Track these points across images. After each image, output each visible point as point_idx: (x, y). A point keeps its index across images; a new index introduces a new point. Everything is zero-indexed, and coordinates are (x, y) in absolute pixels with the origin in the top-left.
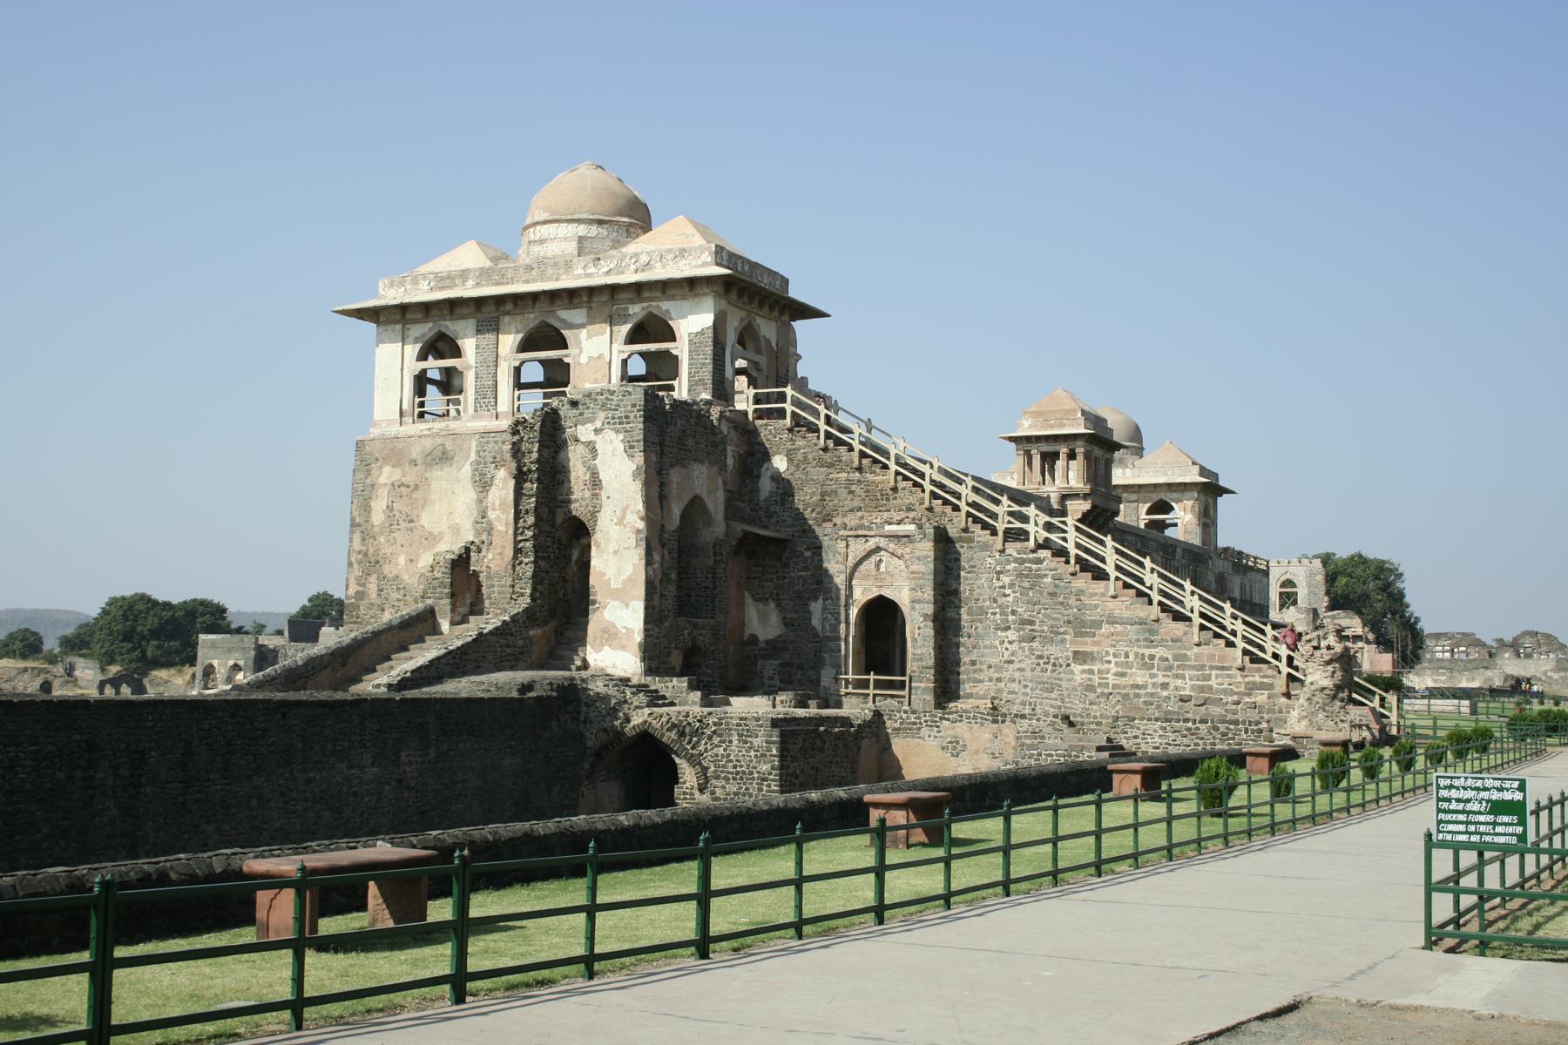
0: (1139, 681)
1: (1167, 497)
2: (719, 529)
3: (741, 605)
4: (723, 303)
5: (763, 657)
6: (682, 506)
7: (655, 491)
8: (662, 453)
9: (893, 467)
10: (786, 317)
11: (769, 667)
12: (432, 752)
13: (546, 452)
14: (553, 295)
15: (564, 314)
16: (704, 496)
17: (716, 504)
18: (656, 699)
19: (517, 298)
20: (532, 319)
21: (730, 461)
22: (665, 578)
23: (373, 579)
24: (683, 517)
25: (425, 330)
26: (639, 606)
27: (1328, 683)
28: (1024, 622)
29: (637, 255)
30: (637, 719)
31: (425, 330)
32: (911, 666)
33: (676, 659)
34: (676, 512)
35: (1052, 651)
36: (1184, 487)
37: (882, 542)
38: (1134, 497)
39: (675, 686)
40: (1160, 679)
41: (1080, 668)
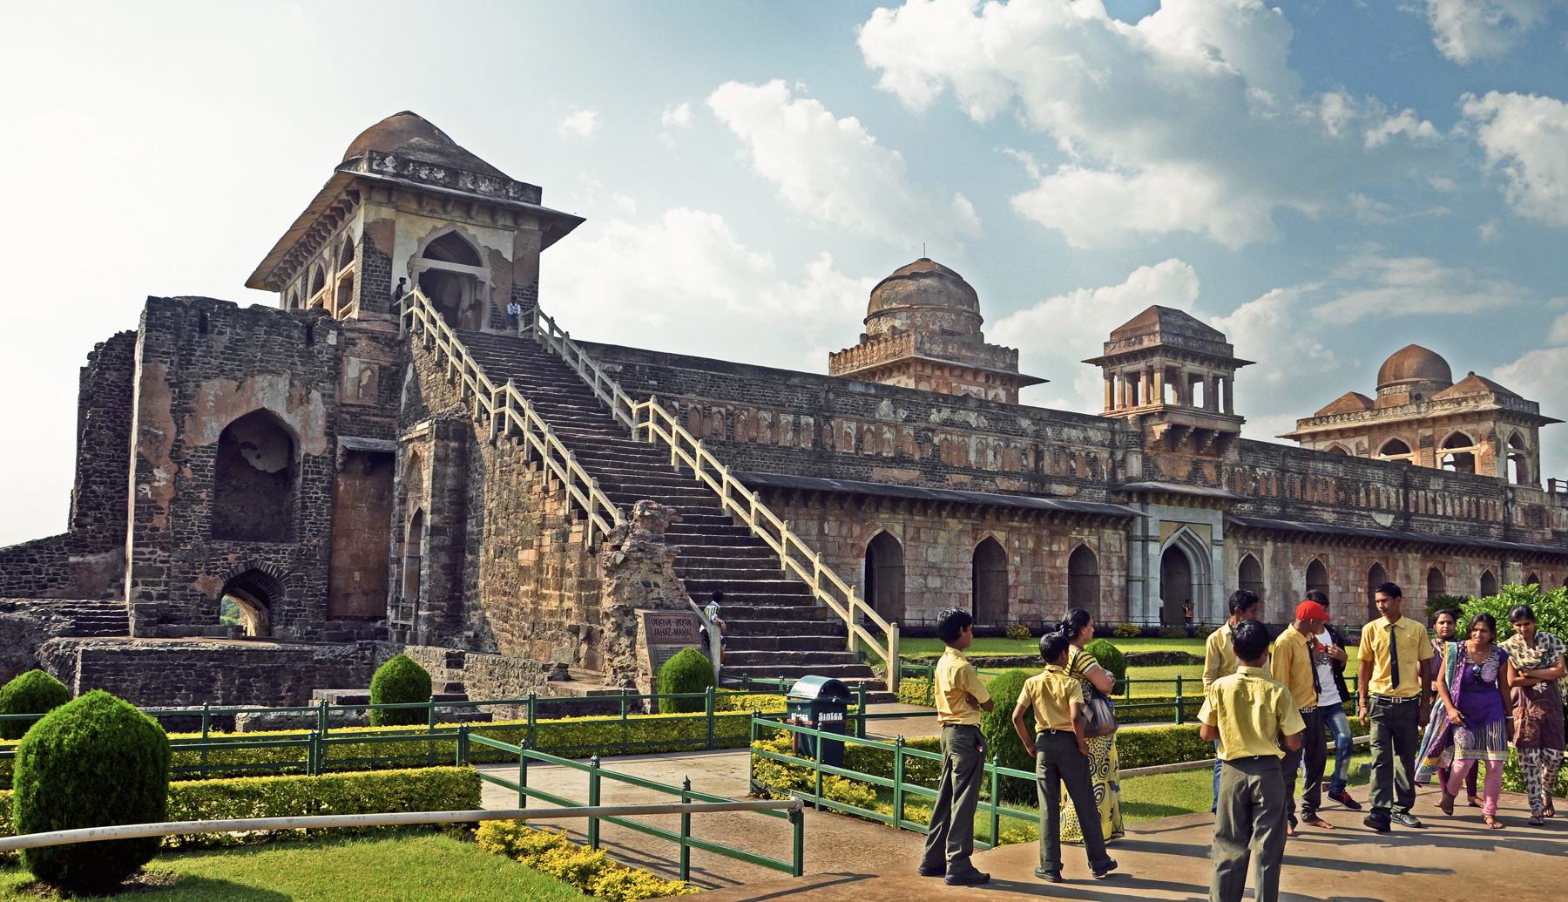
1: (1465, 429)
4: (386, 213)
6: (226, 421)
7: (165, 403)
8: (189, 362)
16: (280, 409)
22: (182, 498)
36: (1480, 416)
41: (523, 588)
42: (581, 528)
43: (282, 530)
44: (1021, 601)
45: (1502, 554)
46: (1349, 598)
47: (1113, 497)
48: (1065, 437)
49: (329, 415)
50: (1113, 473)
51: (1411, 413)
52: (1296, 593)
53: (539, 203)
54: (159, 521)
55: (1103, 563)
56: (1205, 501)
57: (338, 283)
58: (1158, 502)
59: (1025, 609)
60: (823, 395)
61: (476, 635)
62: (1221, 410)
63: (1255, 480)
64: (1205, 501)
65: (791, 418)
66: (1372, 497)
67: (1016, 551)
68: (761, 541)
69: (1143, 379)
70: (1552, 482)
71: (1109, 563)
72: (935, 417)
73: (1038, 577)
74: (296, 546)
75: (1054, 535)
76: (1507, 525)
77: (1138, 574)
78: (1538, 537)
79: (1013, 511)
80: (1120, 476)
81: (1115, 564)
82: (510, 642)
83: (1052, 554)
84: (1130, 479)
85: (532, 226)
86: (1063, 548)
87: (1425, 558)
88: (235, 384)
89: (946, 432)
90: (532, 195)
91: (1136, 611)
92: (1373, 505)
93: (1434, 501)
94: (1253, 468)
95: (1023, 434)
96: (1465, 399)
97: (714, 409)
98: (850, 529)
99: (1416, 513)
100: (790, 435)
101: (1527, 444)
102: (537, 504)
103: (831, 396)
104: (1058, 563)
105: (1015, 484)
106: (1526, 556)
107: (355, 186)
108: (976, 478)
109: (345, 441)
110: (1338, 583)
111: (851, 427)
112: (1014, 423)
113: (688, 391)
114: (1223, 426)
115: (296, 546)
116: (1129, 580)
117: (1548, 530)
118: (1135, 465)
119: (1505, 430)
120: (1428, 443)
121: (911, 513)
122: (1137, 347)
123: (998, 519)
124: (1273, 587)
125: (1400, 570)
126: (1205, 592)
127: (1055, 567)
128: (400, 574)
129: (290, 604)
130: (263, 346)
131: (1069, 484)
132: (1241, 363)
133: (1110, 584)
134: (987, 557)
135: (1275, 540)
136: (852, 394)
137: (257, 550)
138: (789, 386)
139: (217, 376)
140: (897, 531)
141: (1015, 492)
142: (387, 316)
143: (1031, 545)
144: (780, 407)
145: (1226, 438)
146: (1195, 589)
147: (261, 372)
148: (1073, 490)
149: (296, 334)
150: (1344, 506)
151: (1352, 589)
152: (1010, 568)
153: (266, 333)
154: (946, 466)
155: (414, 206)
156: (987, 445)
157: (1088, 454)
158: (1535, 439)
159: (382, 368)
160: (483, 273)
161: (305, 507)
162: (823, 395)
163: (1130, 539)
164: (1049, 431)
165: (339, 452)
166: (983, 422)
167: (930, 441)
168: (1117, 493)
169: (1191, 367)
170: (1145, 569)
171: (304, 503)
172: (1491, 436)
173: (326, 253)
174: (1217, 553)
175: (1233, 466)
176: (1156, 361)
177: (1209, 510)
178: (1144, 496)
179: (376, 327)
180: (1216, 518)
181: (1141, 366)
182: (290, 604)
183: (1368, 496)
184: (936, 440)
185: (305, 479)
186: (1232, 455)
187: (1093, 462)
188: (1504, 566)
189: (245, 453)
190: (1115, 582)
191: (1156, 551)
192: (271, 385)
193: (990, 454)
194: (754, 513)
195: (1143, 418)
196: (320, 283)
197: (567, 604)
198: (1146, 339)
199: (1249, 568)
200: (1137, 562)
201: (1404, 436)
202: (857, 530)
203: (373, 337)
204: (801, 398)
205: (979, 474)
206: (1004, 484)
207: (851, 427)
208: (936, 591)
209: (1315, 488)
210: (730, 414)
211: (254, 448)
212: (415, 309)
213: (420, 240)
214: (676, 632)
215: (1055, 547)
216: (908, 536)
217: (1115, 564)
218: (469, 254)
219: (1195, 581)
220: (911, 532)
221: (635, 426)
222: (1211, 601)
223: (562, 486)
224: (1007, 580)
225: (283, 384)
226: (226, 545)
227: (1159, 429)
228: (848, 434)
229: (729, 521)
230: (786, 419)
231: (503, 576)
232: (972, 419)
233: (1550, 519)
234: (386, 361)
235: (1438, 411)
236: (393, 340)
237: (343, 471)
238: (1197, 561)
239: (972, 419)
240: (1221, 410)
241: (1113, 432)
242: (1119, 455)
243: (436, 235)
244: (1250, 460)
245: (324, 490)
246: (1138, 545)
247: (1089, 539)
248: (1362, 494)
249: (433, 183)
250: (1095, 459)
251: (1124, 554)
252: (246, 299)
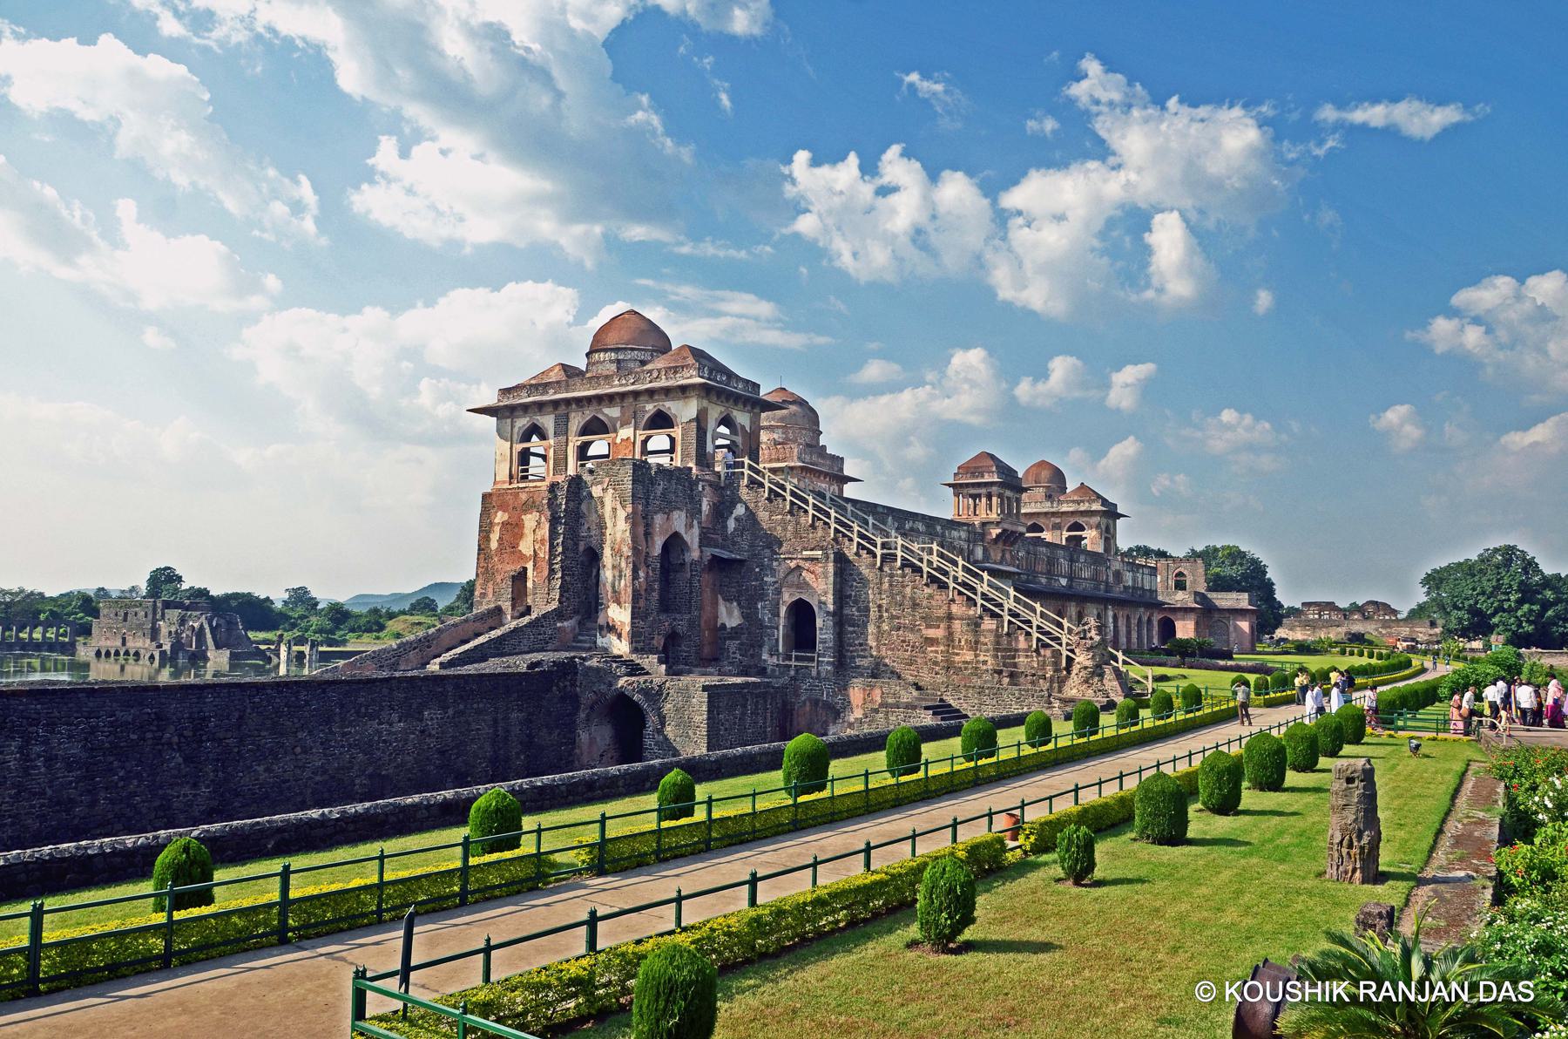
0: (968, 658)
1: (1081, 520)
2: (695, 554)
3: (715, 604)
4: (705, 403)
5: (731, 638)
7: (641, 530)
9: (811, 512)
10: (757, 410)
11: (732, 645)
12: (451, 712)
13: (571, 504)
14: (599, 399)
15: (606, 411)
16: (682, 532)
17: (692, 538)
18: (635, 669)
19: (579, 401)
20: (588, 414)
21: (705, 507)
23: (490, 585)
24: (665, 547)
25: (522, 423)
26: (629, 607)
27: (1089, 663)
28: (892, 617)
29: (650, 372)
30: (621, 682)
31: (522, 423)
32: (819, 647)
33: (659, 641)
34: (659, 542)
35: (911, 637)
37: (802, 563)
39: (650, 661)
40: (981, 658)
51: (1046, 507)
54: (642, 603)
69: (984, 500)
76: (1107, 582)
119: (1104, 521)
120: (1057, 527)
132: (1026, 490)
172: (1098, 526)
176: (994, 489)
181: (983, 491)
195: (984, 524)
201: (1041, 522)
225: (683, 515)
227: (995, 532)
235: (1065, 508)
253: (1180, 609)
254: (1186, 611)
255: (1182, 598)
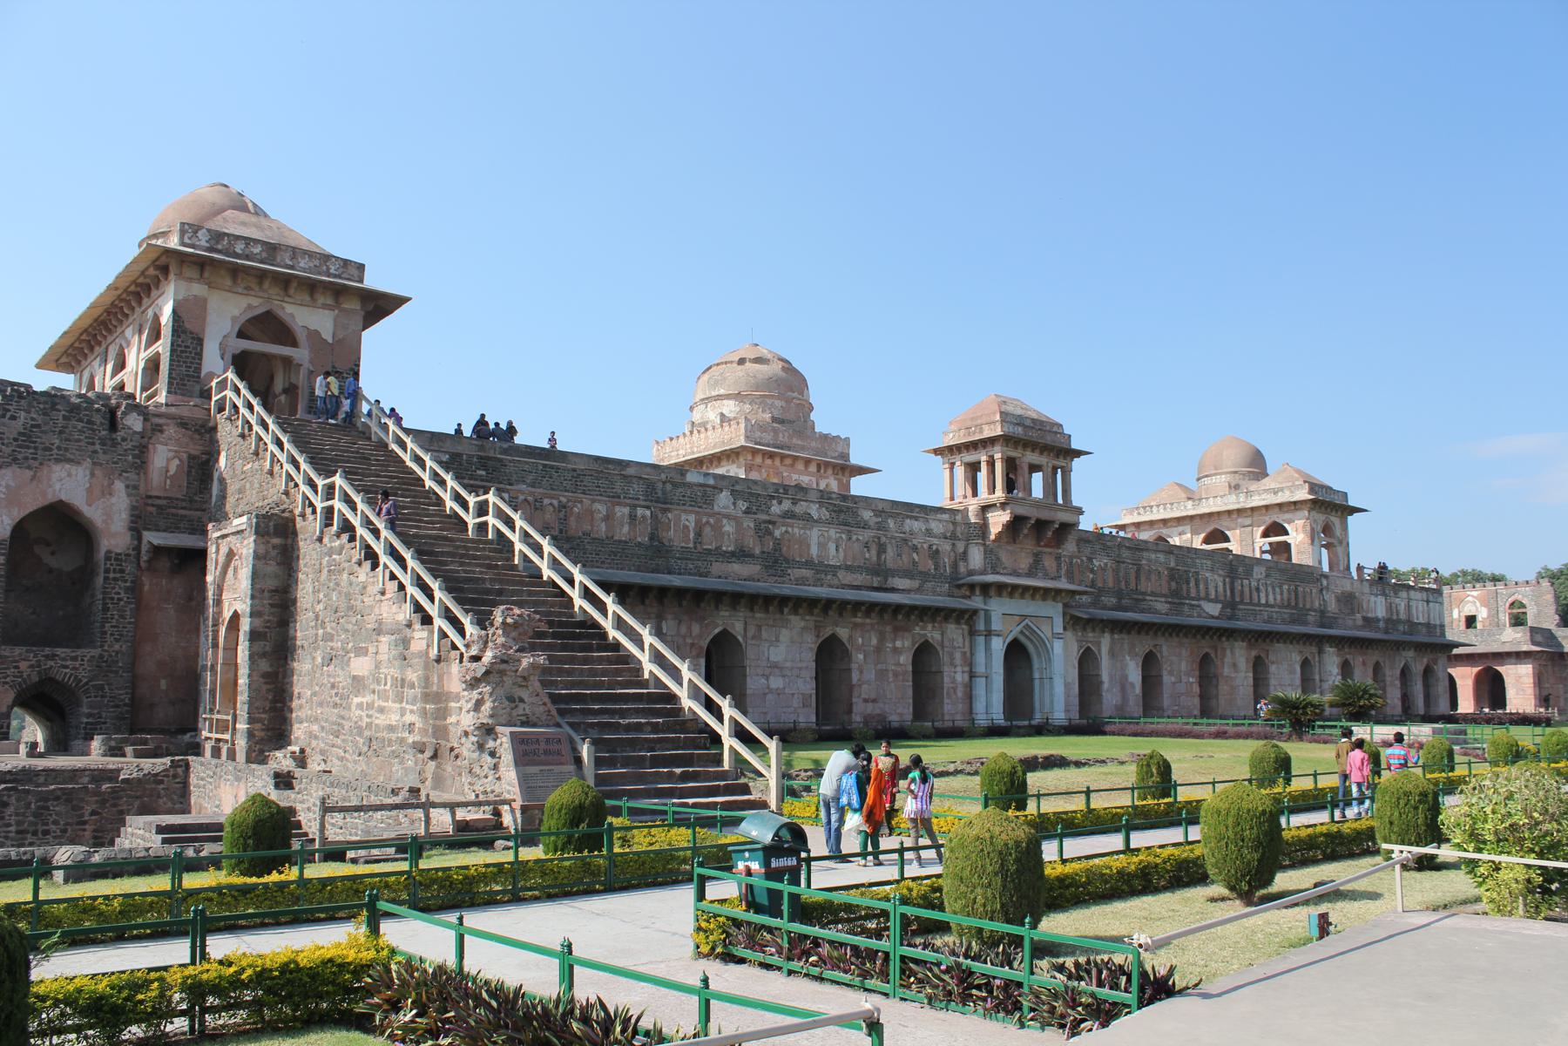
0: (394, 718)
4: (198, 289)
36: (1295, 505)
38: (1248, 521)
41: (356, 700)
42: (425, 634)
43: (75, 632)
44: (866, 701)
45: (1319, 641)
46: (1182, 688)
47: (956, 591)
48: (907, 529)
49: (133, 508)
50: (955, 566)
51: (1232, 502)
52: (1132, 685)
53: (361, 281)
55: (946, 659)
56: (1046, 594)
57: (142, 365)
58: (1000, 595)
59: (870, 708)
60: (660, 485)
61: (302, 751)
62: (1060, 501)
63: (1092, 571)
64: (1046, 594)
65: (626, 510)
66: (1202, 586)
67: (859, 649)
68: (617, 646)
70: (1360, 568)
71: (952, 658)
72: (776, 509)
73: (881, 675)
74: (95, 652)
75: (896, 630)
76: (1323, 613)
77: (980, 668)
78: (1350, 623)
79: (857, 606)
80: (962, 569)
81: (958, 661)
82: (342, 759)
83: (895, 650)
84: (971, 573)
85: (353, 305)
86: (907, 644)
87: (1251, 646)
88: (29, 473)
89: (787, 525)
90: (355, 272)
91: (979, 706)
92: (1202, 594)
93: (1258, 589)
94: (1090, 559)
95: (865, 526)
96: (1282, 489)
97: (546, 501)
98: (689, 628)
99: (1242, 602)
100: (626, 529)
101: (1338, 532)
102: (372, 607)
103: (669, 487)
104: (902, 659)
105: (859, 579)
106: (1341, 642)
107: (164, 260)
108: (818, 572)
109: (153, 538)
110: (1171, 673)
111: (690, 520)
112: (855, 514)
113: (518, 482)
114: (1064, 517)
115: (95, 652)
116: (972, 675)
117: (1358, 616)
118: (976, 557)
121: (752, 610)
122: (977, 437)
123: (841, 614)
124: (1111, 678)
125: (1228, 659)
126: (1047, 687)
127: (899, 664)
128: (214, 683)
129: (89, 715)
130: (61, 432)
131: (912, 578)
132: (1079, 453)
133: (954, 681)
134: (830, 656)
135: (1112, 632)
136: (690, 485)
137: (53, 657)
138: (625, 476)
139: (10, 465)
140: (737, 628)
141: (858, 588)
142: (198, 401)
143: (874, 641)
144: (615, 498)
145: (1067, 528)
146: (1037, 683)
147: (58, 461)
148: (916, 584)
149: (98, 419)
150: (1177, 597)
151: (1184, 679)
152: (854, 666)
153: (65, 418)
154: (787, 560)
155: (229, 282)
156: (829, 538)
157: (930, 547)
158: (1345, 529)
159: (191, 457)
160: (301, 354)
161: (106, 609)
162: (660, 485)
163: (973, 633)
164: (891, 522)
165: (144, 548)
166: (825, 514)
167: (770, 533)
168: (959, 587)
169: (1032, 457)
170: (988, 664)
171: (105, 604)
173: (128, 332)
174: (1058, 646)
175: (1071, 557)
177: (1050, 602)
178: (985, 588)
179: (184, 412)
180: (1054, 610)
182: (89, 715)
183: (1197, 585)
184: (777, 533)
185: (106, 579)
186: (1070, 547)
187: (935, 554)
188: (1320, 652)
189: (37, 549)
190: (959, 678)
191: (998, 646)
192: (69, 475)
193: (832, 546)
194: (611, 616)
195: (985, 509)
196: (121, 365)
197: (409, 718)
198: (986, 428)
199: (1087, 661)
200: (980, 657)
202: (696, 629)
203: (183, 424)
204: (637, 489)
205: (821, 569)
206: (846, 577)
207: (690, 520)
208: (778, 692)
209: (1148, 579)
210: (563, 506)
211: (48, 545)
212: (229, 393)
213: (234, 319)
214: (546, 752)
215: (898, 644)
216: (750, 634)
217: (958, 661)
218: (285, 334)
219: (1036, 675)
220: (752, 631)
221: (471, 520)
222: (1052, 695)
223: (402, 587)
224: (850, 677)
226: (17, 650)
227: (998, 521)
228: (686, 527)
229: (582, 624)
230: (622, 511)
231: (333, 686)
232: (814, 510)
233: (1360, 605)
234: (195, 449)
235: (1256, 501)
236: (203, 426)
237: (148, 569)
238: (1039, 656)
239: (814, 510)
240: (1060, 501)
241: (954, 523)
242: (960, 546)
243: (250, 315)
244: (1087, 551)
245: (127, 590)
246: (982, 639)
247: (932, 633)
248: (1192, 584)
249: (247, 258)
250: (937, 551)
251: (967, 649)
252: (43, 381)
253: (1509, 654)
254: (1519, 657)
255: (1513, 638)
